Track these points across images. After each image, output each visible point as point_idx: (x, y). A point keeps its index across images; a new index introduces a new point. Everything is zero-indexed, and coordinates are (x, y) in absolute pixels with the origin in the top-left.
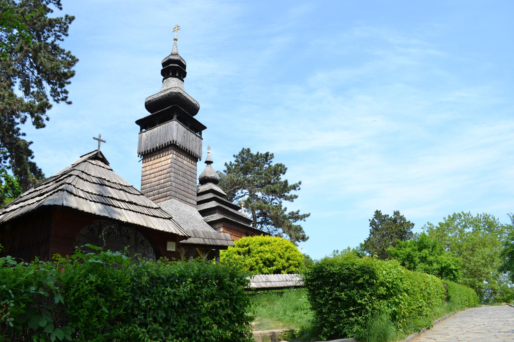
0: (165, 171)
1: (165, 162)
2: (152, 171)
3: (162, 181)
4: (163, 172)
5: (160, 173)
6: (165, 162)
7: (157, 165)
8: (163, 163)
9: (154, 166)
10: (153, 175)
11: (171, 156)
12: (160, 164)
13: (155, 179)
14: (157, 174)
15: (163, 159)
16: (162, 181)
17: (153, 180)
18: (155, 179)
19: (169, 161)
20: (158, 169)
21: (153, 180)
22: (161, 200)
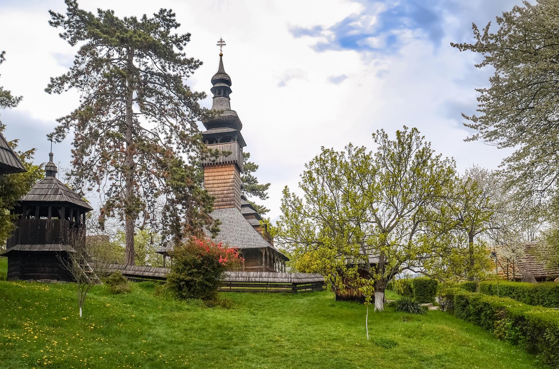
0: (229, 184)
1: (228, 177)
2: (215, 182)
3: (226, 192)
4: (226, 185)
5: (223, 185)
6: (228, 177)
7: (219, 177)
8: (226, 177)
9: (216, 178)
10: (216, 185)
11: (233, 172)
12: (223, 177)
13: (219, 189)
14: (220, 185)
15: (225, 173)
16: (226, 192)
17: (216, 189)
18: (219, 189)
19: (232, 177)
20: (221, 181)
21: (216, 189)
22: (225, 207)
